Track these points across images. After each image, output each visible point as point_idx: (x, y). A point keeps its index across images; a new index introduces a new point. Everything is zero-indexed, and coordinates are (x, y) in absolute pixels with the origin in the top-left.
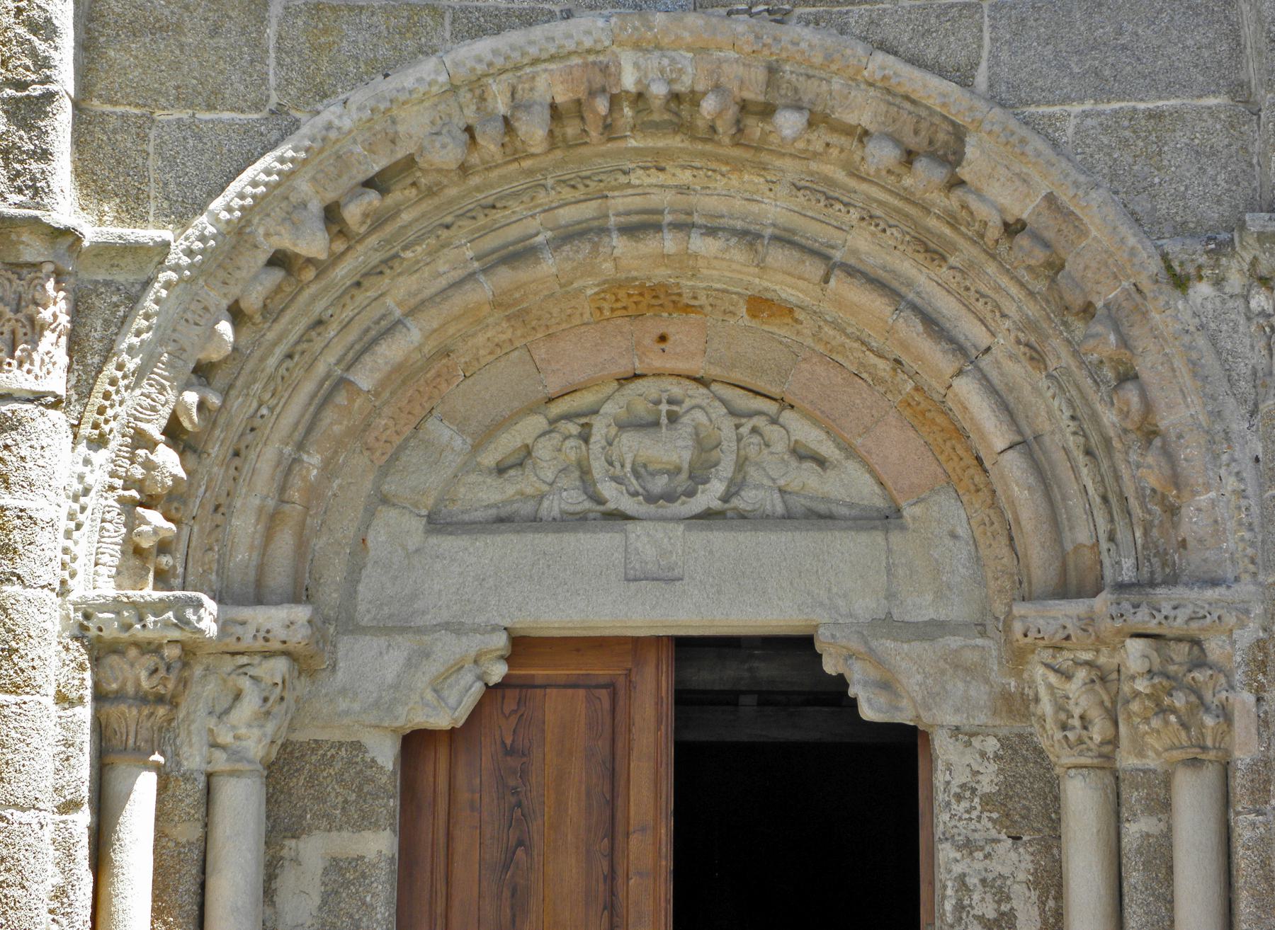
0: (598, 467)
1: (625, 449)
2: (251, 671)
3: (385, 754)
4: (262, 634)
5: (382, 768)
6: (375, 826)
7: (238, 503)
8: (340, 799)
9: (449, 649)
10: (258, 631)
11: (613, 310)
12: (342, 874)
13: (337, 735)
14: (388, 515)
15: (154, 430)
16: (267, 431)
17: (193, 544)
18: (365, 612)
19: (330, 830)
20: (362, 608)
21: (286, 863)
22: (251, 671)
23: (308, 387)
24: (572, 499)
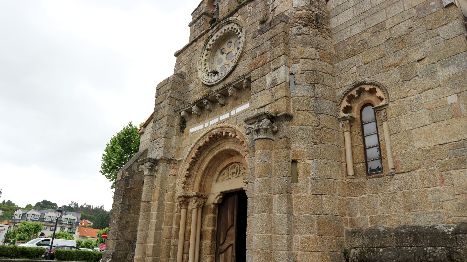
3: (212, 206)
9: (217, 195)
12: (209, 218)
15: (184, 176)
24: (227, 178)
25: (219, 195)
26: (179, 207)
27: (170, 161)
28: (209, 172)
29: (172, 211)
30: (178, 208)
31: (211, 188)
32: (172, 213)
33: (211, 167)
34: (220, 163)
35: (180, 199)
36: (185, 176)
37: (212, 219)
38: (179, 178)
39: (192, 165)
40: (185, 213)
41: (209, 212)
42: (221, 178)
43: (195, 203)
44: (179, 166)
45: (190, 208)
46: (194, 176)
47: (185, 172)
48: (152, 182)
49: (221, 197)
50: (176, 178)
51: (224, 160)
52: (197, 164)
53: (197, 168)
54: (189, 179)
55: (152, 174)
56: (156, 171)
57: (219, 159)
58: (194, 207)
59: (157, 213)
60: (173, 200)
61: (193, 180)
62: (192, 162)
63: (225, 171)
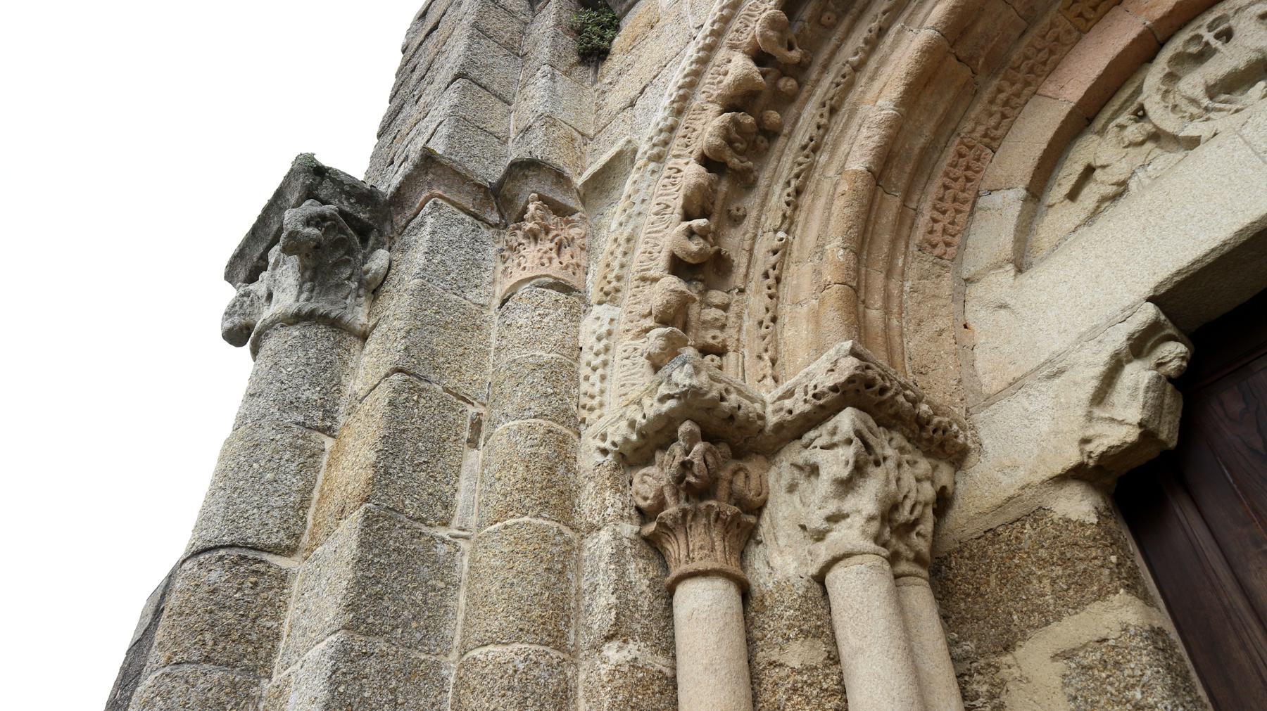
0: (1170, 123)
1: (1189, 93)
2: (819, 442)
3: (1079, 506)
4: (811, 393)
5: (1082, 525)
6: (1101, 595)
7: (785, 318)
8: (1046, 581)
10: (806, 393)
11: (1094, 8)
13: (1013, 512)
14: (975, 291)
16: (795, 254)
17: (746, 364)
18: (990, 384)
19: (1047, 623)
20: (986, 380)
21: (1011, 687)
22: (819, 442)
23: (821, 203)
25: (1140, 345)
26: (639, 575)
27: (512, 196)
28: (906, 219)
29: (554, 623)
30: (622, 586)
31: (964, 350)
32: (557, 640)
33: (923, 166)
34: (1009, 111)
35: (651, 481)
36: (677, 266)
37: (1142, 662)
38: (610, 296)
39: (731, 170)
40: (738, 639)
41: (1043, 588)
42: (1060, 216)
43: (846, 485)
44: (593, 234)
45: (781, 562)
46: (763, 259)
47: (670, 235)
48: (328, 378)
49: (1173, 352)
50: (575, 316)
51: (1047, 63)
52: (783, 163)
53: (779, 198)
54: (717, 296)
55: (323, 306)
56: (375, 289)
57: (996, 64)
58: (850, 534)
59: (344, 653)
60: (554, 489)
61: (756, 301)
62: (730, 136)
63: (1088, 150)
